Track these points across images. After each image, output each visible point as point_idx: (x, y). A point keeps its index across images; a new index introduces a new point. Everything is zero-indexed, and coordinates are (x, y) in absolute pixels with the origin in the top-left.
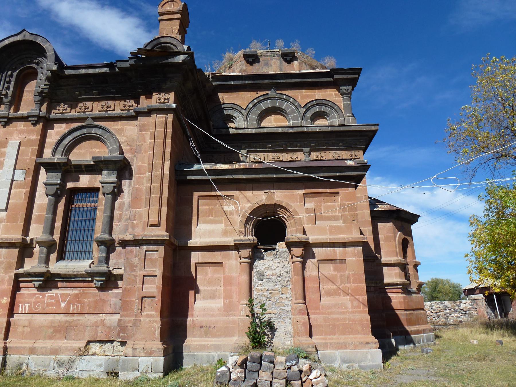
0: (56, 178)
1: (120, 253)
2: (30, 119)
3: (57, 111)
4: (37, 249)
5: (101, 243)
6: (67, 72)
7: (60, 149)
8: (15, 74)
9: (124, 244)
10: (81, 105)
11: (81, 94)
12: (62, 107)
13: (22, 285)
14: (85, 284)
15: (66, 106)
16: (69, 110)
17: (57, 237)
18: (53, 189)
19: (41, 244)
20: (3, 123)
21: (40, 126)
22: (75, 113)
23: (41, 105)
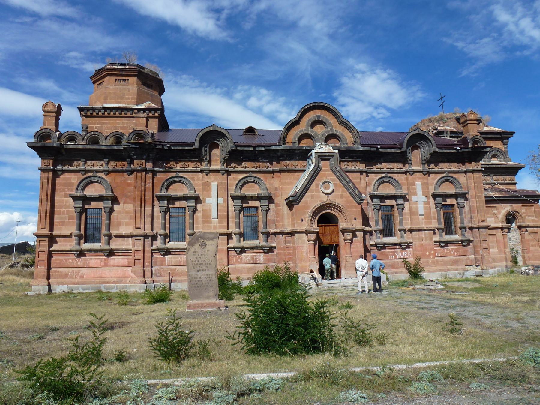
0: (239, 202)
1: (272, 238)
2: (221, 172)
3: (231, 167)
4: (234, 236)
5: (263, 234)
6: (239, 148)
7: (238, 187)
8: (208, 146)
9: (275, 234)
10: (243, 164)
11: (243, 159)
12: (234, 164)
13: (230, 252)
14: (258, 251)
15: (236, 164)
16: (237, 166)
17: (242, 230)
18: (238, 208)
19: (235, 234)
20: (206, 174)
21: (225, 176)
22: (239, 168)
23: (224, 163)
